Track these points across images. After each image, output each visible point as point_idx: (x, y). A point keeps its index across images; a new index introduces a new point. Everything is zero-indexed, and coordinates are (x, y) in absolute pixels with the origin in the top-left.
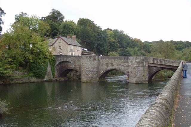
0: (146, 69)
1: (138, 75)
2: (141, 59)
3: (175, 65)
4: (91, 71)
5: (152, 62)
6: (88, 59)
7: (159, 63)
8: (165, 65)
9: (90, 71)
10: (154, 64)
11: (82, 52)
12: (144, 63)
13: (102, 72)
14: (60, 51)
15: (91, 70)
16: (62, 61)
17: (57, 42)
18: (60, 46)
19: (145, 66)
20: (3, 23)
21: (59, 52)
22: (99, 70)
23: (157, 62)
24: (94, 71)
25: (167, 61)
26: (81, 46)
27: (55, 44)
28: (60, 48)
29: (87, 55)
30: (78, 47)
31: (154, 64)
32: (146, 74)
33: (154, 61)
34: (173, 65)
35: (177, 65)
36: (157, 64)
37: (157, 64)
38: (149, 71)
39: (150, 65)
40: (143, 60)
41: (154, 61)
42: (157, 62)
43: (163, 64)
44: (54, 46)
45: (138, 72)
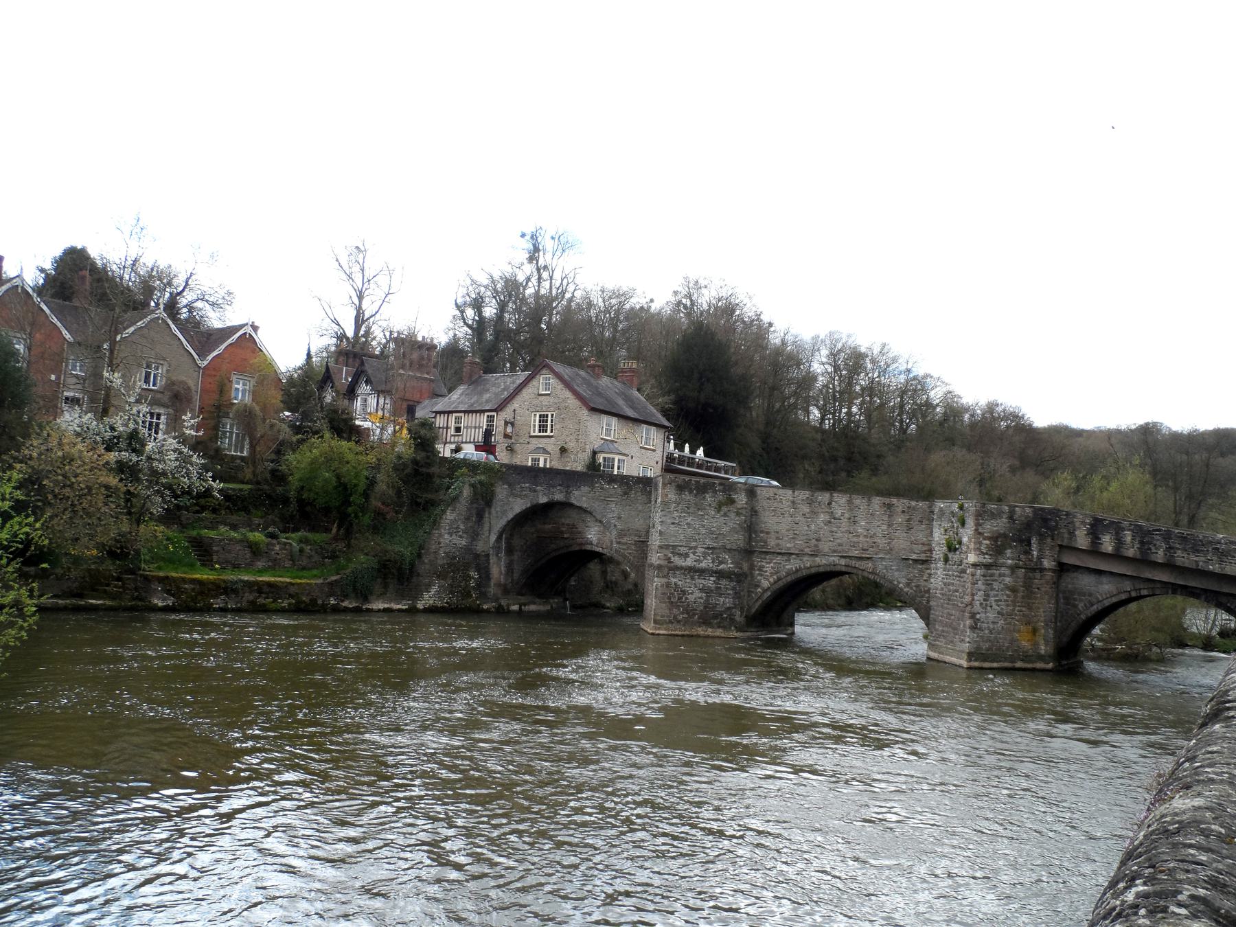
0: (1043, 584)
1: (991, 615)
2: (1011, 518)
4: (702, 572)
5: (1082, 541)
6: (687, 497)
7: (1131, 553)
8: (1170, 566)
9: (693, 571)
11: (670, 458)
12: (1034, 540)
13: (765, 584)
14: (542, 443)
15: (703, 565)
16: (543, 500)
17: (527, 393)
18: (543, 418)
21: (532, 447)
22: (752, 567)
23: (1119, 542)
24: (720, 575)
26: (666, 423)
27: (515, 404)
28: (543, 428)
29: (687, 478)
30: (645, 427)
31: (1095, 551)
32: (1044, 608)
36: (1117, 556)
38: (1065, 599)
39: (1069, 559)
40: (1028, 525)
42: (1119, 542)
44: (507, 414)
45: (987, 596)
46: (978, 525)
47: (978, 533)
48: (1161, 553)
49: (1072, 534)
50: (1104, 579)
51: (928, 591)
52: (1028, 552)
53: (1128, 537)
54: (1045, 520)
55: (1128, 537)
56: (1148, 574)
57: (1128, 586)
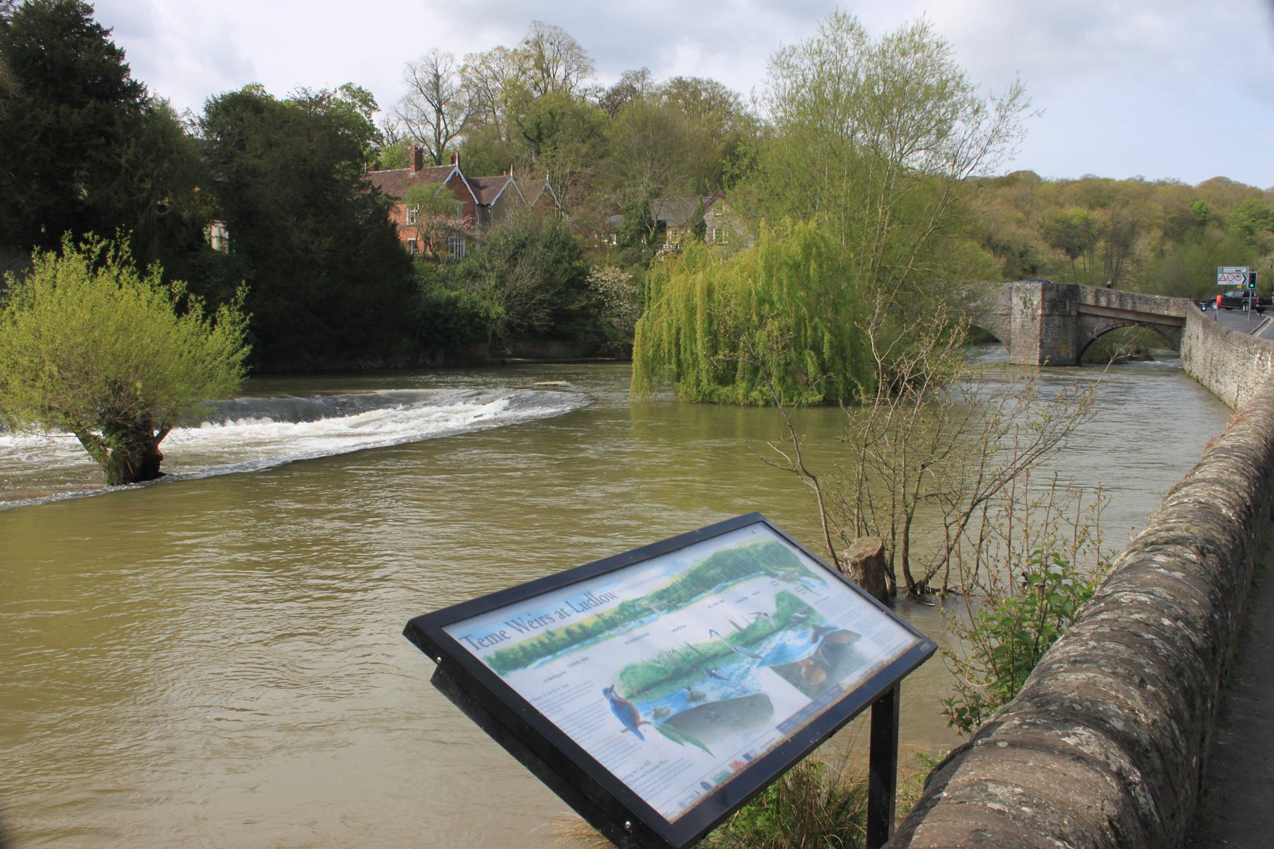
1: (1049, 340)
3: (1166, 313)
7: (1115, 306)
8: (1133, 312)
10: (1097, 307)
19: (1070, 312)
20: (89, 10)
23: (1109, 301)
25: (1140, 298)
33: (1097, 299)
34: (1161, 312)
35: (1173, 314)
37: (1108, 308)
39: (1083, 310)
40: (1065, 294)
41: (1097, 299)
42: (1109, 301)
43: (1129, 307)
46: (1043, 295)
47: (1043, 299)
48: (1129, 305)
49: (1085, 297)
50: (1101, 319)
51: (1010, 331)
52: (1065, 307)
53: (1113, 298)
54: (1072, 291)
55: (1113, 298)
56: (1122, 316)
57: (1111, 322)
